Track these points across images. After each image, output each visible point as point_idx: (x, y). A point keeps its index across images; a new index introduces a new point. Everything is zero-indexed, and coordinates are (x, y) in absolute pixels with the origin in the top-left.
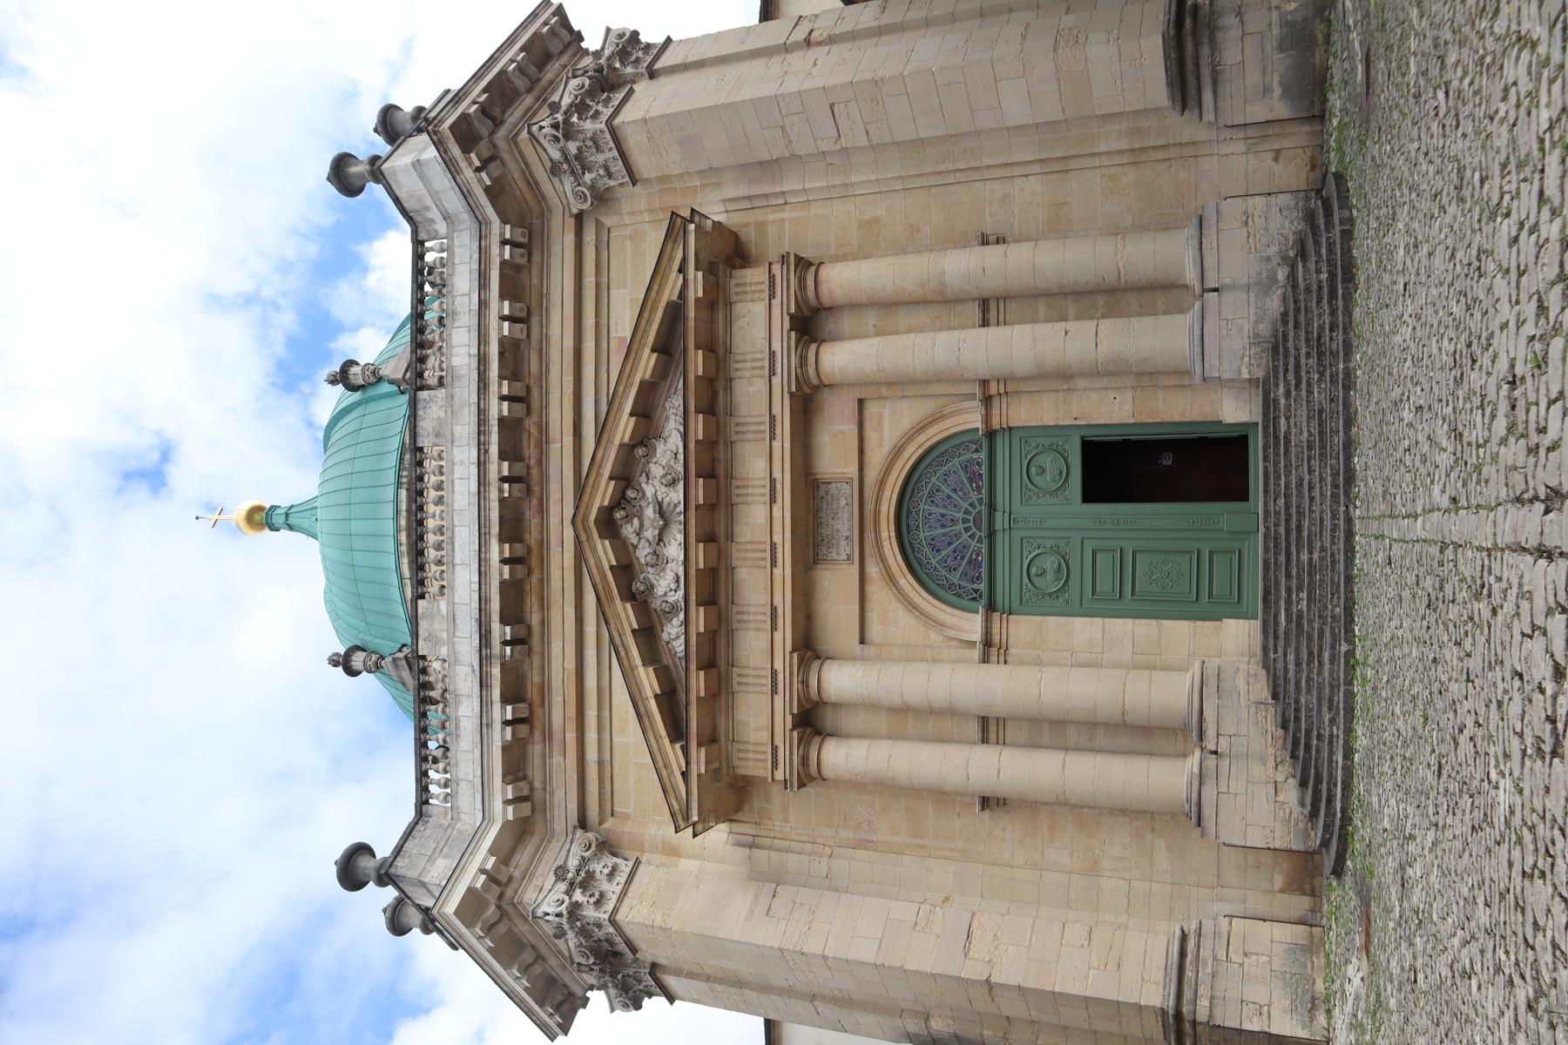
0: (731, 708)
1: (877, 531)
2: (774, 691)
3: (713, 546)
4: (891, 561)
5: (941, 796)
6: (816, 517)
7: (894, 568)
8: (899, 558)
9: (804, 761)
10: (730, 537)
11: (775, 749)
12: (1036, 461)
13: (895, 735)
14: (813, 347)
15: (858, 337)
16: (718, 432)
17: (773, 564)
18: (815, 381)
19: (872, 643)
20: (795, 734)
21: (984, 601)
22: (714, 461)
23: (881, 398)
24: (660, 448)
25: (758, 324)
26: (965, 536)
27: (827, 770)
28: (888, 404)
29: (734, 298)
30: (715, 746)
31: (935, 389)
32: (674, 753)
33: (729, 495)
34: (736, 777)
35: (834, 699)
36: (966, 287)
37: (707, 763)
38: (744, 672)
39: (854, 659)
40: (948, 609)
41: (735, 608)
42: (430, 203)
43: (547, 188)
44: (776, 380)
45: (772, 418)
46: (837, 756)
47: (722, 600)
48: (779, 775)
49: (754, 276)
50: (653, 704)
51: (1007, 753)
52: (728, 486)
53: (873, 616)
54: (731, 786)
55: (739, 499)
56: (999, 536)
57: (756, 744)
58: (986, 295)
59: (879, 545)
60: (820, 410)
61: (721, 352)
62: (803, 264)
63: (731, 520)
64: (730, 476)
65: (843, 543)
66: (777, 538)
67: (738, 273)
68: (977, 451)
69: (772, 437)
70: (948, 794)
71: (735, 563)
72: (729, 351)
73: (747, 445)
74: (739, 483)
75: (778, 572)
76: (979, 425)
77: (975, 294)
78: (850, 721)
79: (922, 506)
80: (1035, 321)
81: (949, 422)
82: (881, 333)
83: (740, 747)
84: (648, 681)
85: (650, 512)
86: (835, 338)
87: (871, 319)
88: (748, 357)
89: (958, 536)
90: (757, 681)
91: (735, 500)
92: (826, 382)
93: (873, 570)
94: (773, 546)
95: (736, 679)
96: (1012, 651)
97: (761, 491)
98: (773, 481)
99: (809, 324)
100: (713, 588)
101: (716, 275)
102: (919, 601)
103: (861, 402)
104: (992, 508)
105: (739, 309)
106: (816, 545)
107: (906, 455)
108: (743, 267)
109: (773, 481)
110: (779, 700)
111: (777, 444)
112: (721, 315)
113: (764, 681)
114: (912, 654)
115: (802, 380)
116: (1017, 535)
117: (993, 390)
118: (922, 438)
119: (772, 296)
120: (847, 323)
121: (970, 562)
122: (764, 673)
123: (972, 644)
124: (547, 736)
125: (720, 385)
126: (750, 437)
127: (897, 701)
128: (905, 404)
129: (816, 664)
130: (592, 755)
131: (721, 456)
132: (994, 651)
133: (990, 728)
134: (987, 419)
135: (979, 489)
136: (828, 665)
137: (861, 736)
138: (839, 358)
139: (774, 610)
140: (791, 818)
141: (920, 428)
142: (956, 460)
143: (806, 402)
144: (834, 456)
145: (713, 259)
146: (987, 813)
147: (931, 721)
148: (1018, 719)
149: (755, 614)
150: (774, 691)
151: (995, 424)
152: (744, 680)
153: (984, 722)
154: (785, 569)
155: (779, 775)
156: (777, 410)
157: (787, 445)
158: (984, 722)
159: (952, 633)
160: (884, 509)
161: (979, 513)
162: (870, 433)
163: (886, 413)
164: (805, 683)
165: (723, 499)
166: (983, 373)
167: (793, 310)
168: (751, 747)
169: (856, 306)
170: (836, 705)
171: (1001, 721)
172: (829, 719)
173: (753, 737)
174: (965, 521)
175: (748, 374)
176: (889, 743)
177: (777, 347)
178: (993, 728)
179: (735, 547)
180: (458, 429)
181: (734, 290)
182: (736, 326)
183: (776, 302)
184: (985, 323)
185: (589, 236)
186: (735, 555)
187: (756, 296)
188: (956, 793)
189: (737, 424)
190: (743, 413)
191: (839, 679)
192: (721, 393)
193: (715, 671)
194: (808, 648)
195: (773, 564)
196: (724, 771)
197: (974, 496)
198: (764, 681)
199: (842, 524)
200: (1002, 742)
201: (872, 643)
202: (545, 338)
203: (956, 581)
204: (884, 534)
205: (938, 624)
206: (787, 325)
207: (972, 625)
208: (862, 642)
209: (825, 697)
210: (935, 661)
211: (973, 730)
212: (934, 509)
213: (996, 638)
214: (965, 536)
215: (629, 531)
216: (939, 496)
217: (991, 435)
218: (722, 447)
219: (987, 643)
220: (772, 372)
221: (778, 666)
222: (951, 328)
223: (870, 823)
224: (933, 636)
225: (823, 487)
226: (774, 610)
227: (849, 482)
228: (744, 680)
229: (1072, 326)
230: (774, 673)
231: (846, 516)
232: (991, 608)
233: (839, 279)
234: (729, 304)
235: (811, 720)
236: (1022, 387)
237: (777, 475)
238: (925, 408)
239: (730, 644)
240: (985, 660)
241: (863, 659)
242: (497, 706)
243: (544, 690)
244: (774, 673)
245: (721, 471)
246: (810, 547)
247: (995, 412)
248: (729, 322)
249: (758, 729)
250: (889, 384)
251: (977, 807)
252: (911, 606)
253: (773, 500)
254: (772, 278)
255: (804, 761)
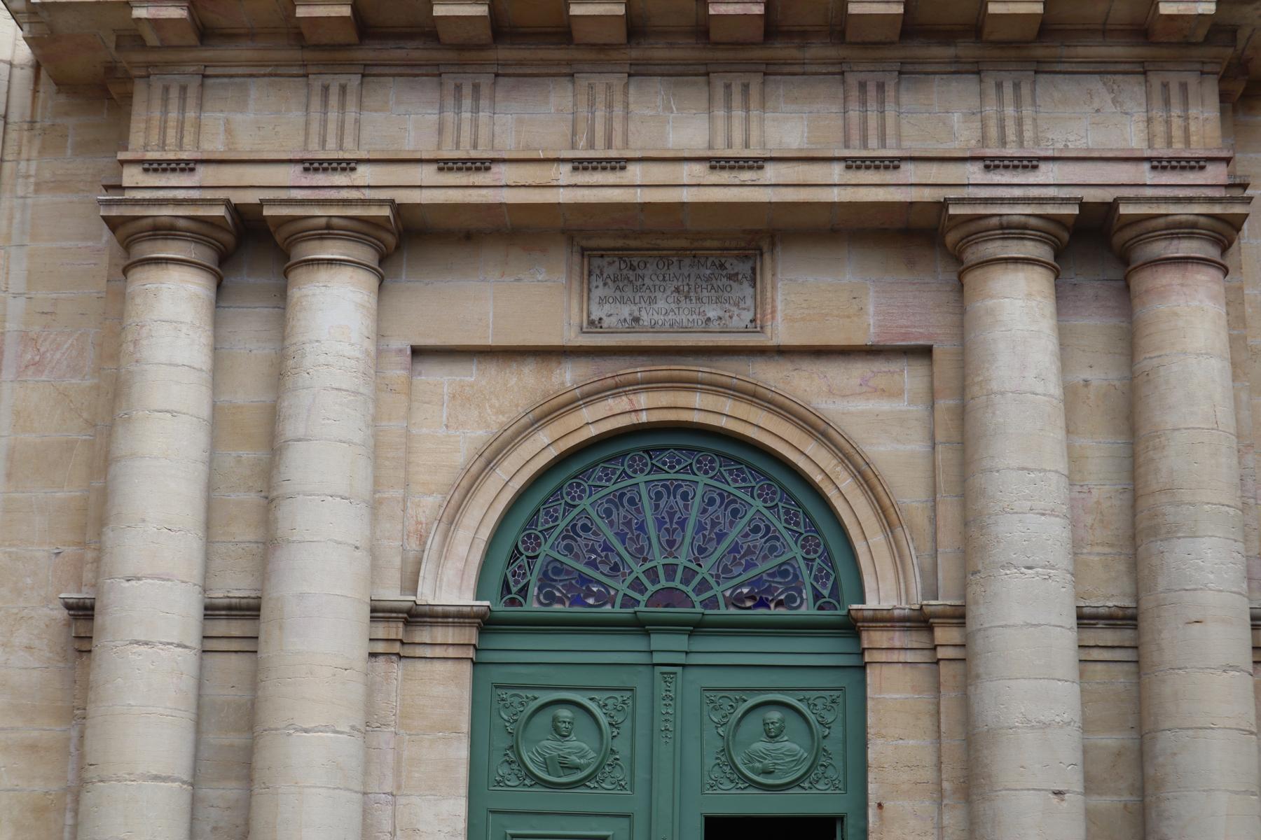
0: (274, 72)
1: (651, 384)
2: (311, 165)
3: (619, 35)
4: (587, 414)
5: (95, 521)
6: (681, 253)
7: (572, 421)
8: (593, 431)
9: (163, 231)
10: (639, 71)
11: (187, 166)
12: (793, 723)
13: (219, 422)
14: (1042, 251)
15: (1063, 346)
16: (865, 45)
17: (581, 164)
18: (972, 255)
19: (412, 371)
20: (220, 211)
21: (501, 609)
22: (802, 36)
23: (932, 396)
26: (638, 570)
28: (919, 410)
29: (1156, 80)
30: (192, 39)
31: (948, 511)
33: (730, 67)
34: (129, 79)
35: (295, 293)
36: (1162, 583)
37: (155, 23)
38: (351, 100)
39: (380, 335)
40: (485, 533)
41: (485, 80)
44: (974, 173)
45: (893, 163)
46: (175, 301)
47: (504, 53)
48: (132, 176)
49: (1201, 123)
51: (187, 660)
52: (748, 67)
53: (470, 375)
54: (110, 69)
55: (720, 92)
56: (637, 643)
57: (198, 126)
58: (1143, 625)
59: (619, 388)
60: (911, 264)
61: (1039, 52)
62: (1224, 233)
63: (676, 72)
64: (770, 70)
65: (625, 311)
66: (635, 173)
67: (1211, 91)
68: (817, 596)
69: (852, 163)
70: (100, 534)
71: (583, 81)
72: (1041, 68)
73: (836, 108)
74: (754, 91)
75: (564, 174)
76: (872, 603)
77: (1147, 603)
78: (250, 330)
79: (702, 479)
80: (1087, 726)
81: (878, 539)
82: (1071, 396)
83: (192, 93)
86: (1062, 297)
87: (1099, 374)
88: (1027, 111)
89: (641, 555)
90: (332, 127)
91: (718, 82)
92: (970, 278)
93: (568, 376)
94: (618, 164)
95: (335, 82)
96: (397, 669)
97: (738, 136)
98: (757, 163)
99: (1097, 247)
101: (1207, 41)
102: (501, 473)
103: (924, 352)
104: (697, 628)
105: (1133, 91)
106: (621, 254)
107: (811, 447)
108: (1224, 97)
109: (757, 163)
110: (291, 175)
111: (836, 172)
112: (1119, 51)
113: (331, 143)
114: (386, 456)
115: (979, 228)
116: (640, 680)
117: (943, 635)
118: (846, 482)
119: (1159, 164)
120: (1095, 324)
121: (585, 580)
122: (349, 142)
123: (412, 583)
125: (965, 50)
126: (854, 115)
127: (292, 428)
128: (916, 446)
129: (366, 254)
131: (816, 51)
132: (397, 630)
133: (236, 620)
134: (884, 620)
135: (737, 601)
136: (373, 281)
137: (217, 350)
138: (1020, 310)
139: (482, 165)
140: (45, 198)
141: (866, 479)
142: (798, 552)
143: (930, 239)
144: (808, 298)
145: (1243, 35)
146: (63, 614)
147: (252, 497)
148: (255, 681)
149: (475, 125)
150: (311, 165)
151: (874, 638)
152: (334, 100)
153: (250, 610)
154: (568, 189)
155: (132, 176)
156: (909, 173)
157: (835, 196)
158: (250, 610)
159: (433, 542)
160: (697, 400)
161: (686, 601)
162: (857, 371)
163: (901, 405)
164: (328, 231)
165: (719, 55)
166: (979, 615)
167: (1124, 210)
168: (191, 115)
169: (1130, 343)
170: (281, 298)
171: (251, 646)
172: (248, 279)
173: (214, 119)
174: (670, 570)
175: (991, 109)
176: (205, 411)
177: (1048, 173)
178: (236, 628)
179: (617, 80)
181: (1174, 79)
182: (1095, 83)
183: (1144, 173)
184: (1085, 619)
186: (600, 82)
187: (1160, 129)
188: (100, 550)
189: (881, 87)
190: (905, 98)
191: (336, 306)
192: (950, 52)
193: (350, 36)
194: (404, 241)
195: (581, 164)
196: (138, 57)
197: (722, 590)
198: (331, 143)
199: (666, 314)
200: (208, 647)
201: (412, 371)
203: (545, 549)
204: (643, 400)
205: (452, 516)
206: (1091, 196)
207: (452, 585)
208: (418, 353)
209: (299, 275)
210: (375, 507)
211: (235, 587)
212: (696, 504)
213: (423, 635)
214: (638, 570)
216: (724, 520)
217: (851, 628)
218: (832, 52)
219: (414, 617)
220: (991, 164)
221: (364, 175)
222: (1076, 547)
223: (38, 365)
224: (428, 505)
225: (745, 268)
226: (482, 165)
227: (756, 325)
228: (334, 100)
229: (1074, 803)
230: (348, 165)
231: (683, 317)
232: (487, 624)
233: (1190, 314)
234: (1143, 69)
235: (251, 248)
236: (949, 698)
237: (771, 173)
238: (909, 491)
239: (410, 71)
240: (379, 613)
241: (380, 353)
244: (348, 165)
245: (781, 51)
246: (616, 244)
247: (898, 638)
248: (1102, 69)
249: (229, 131)
250: (962, 414)
251: (73, 595)
252: (492, 456)
253: (716, 163)
254: (1197, 164)
255: (163, 231)
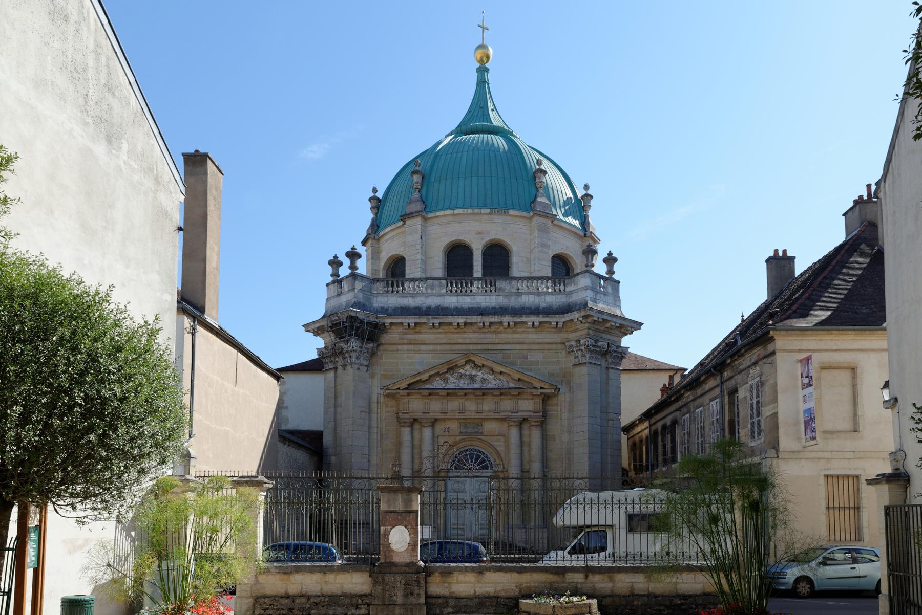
9: (405, 422)
24: (492, 377)
25: (527, 406)
27: (402, 429)
32: (404, 385)
42: (576, 287)
43: (574, 334)
50: (418, 378)
84: (425, 377)
85: (474, 373)
100: (451, 393)
124: (405, 334)
130: (399, 347)
180: (501, 298)
185: (560, 346)
202: (528, 333)
215: (468, 367)
242: (414, 321)
243: (419, 332)
